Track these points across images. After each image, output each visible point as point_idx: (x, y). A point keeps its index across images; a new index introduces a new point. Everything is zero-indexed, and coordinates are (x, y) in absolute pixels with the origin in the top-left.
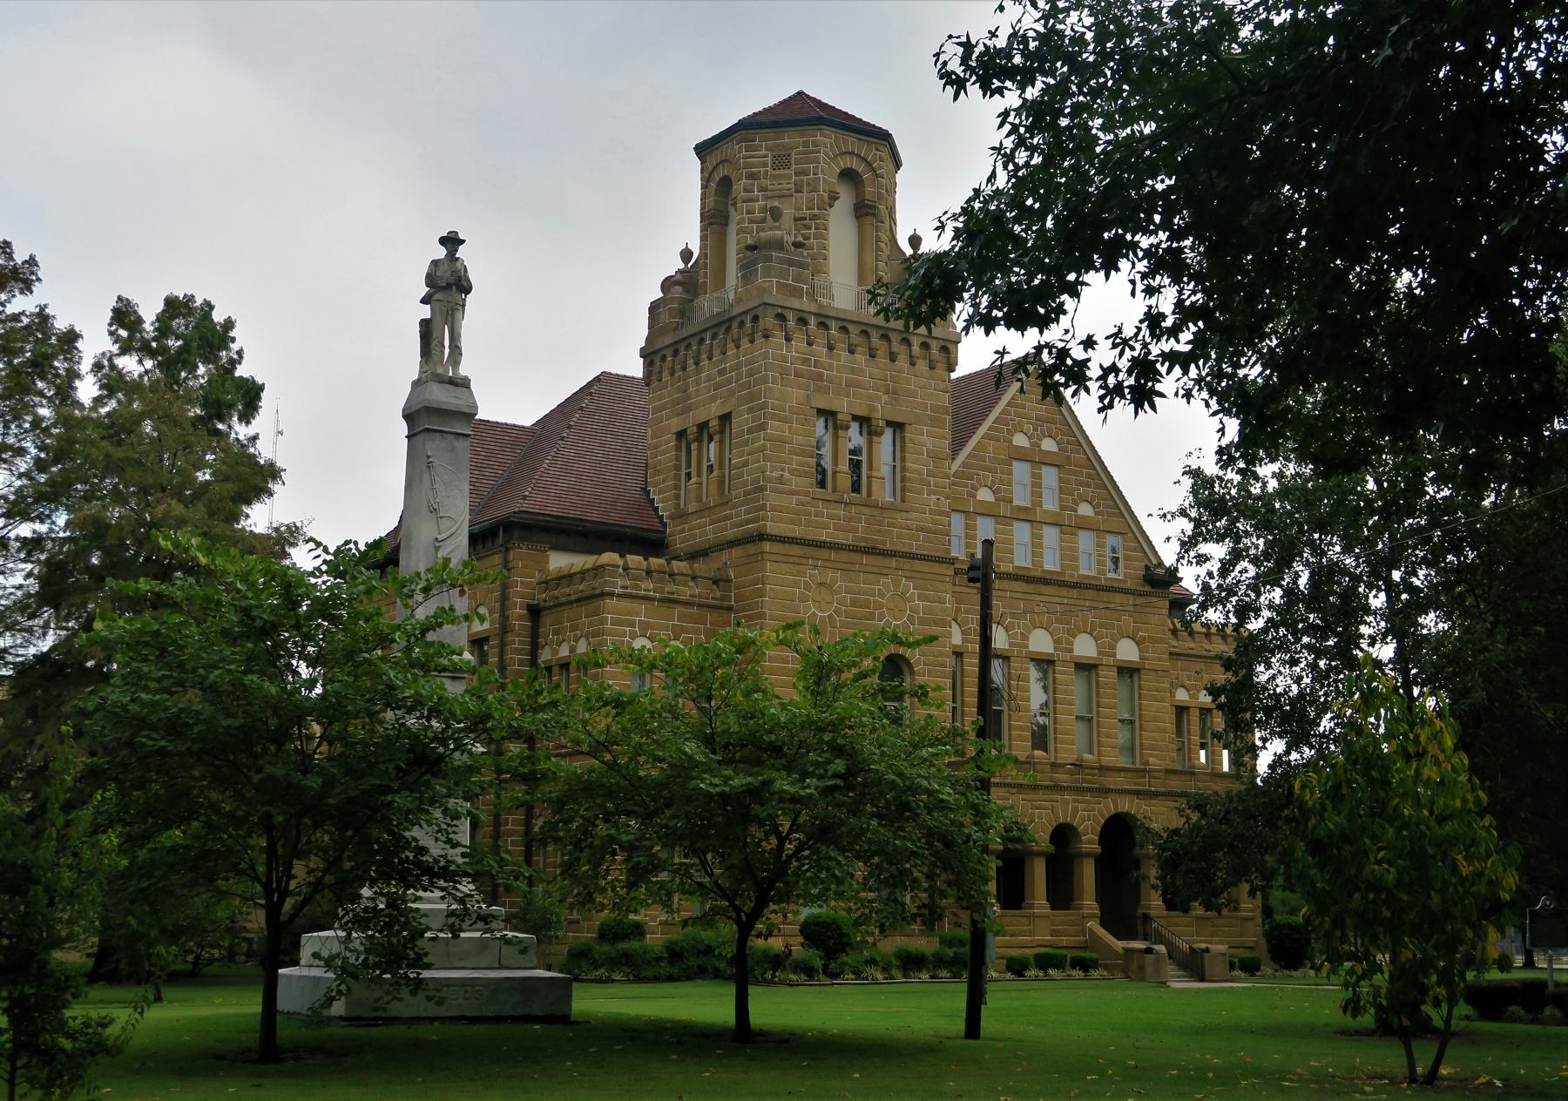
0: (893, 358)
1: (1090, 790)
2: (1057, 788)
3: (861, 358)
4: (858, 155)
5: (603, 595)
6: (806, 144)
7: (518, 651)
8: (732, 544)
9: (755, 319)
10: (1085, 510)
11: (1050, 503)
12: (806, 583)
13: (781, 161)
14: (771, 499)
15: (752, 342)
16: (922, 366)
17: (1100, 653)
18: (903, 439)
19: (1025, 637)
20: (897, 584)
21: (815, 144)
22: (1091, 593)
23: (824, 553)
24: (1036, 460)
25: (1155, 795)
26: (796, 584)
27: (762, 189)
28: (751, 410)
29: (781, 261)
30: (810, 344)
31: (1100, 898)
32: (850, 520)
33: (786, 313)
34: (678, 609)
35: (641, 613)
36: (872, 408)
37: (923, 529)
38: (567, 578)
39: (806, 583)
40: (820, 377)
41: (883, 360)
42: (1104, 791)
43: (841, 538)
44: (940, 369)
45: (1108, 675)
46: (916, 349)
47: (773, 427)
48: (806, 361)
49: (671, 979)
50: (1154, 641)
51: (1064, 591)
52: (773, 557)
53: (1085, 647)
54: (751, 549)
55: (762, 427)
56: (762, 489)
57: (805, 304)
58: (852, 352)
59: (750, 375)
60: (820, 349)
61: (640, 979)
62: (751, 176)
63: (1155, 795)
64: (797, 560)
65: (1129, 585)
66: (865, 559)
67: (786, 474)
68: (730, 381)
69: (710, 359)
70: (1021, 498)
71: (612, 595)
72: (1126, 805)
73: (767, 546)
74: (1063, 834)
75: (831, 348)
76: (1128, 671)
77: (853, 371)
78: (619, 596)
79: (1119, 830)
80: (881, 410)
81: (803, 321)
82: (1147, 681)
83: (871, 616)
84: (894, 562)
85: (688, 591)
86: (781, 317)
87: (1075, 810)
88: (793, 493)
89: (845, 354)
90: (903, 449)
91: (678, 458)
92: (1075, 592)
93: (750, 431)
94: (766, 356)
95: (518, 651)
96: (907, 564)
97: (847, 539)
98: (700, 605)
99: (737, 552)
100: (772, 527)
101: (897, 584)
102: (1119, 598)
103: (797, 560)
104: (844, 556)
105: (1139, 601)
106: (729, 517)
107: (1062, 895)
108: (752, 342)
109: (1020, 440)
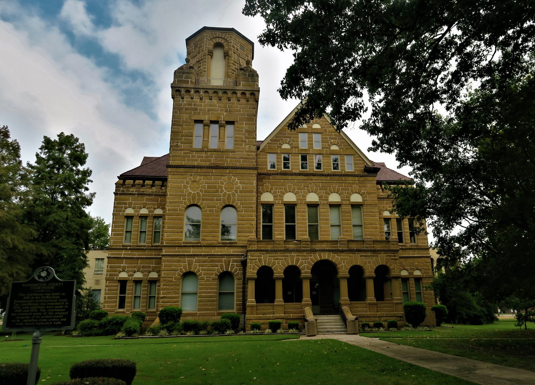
3: (215, 101)
4: (221, 38)
10: (334, 148)
12: (187, 182)
17: (342, 200)
20: (229, 179)
23: (196, 170)
25: (343, 251)
26: (182, 182)
30: (192, 98)
31: (312, 297)
32: (207, 157)
33: (180, 89)
34: (146, 197)
36: (219, 117)
37: (242, 158)
39: (187, 182)
41: (224, 101)
43: (203, 164)
51: (323, 178)
52: (172, 173)
57: (189, 85)
58: (211, 99)
63: (343, 251)
64: (183, 173)
65: (357, 173)
67: (179, 144)
72: (325, 256)
75: (201, 99)
76: (356, 206)
77: (211, 106)
78: (120, 194)
81: (188, 91)
83: (217, 191)
84: (228, 171)
85: (150, 191)
87: (298, 260)
88: (181, 150)
89: (208, 101)
96: (234, 171)
98: (155, 195)
101: (229, 179)
103: (183, 173)
104: (204, 170)
105: (361, 179)
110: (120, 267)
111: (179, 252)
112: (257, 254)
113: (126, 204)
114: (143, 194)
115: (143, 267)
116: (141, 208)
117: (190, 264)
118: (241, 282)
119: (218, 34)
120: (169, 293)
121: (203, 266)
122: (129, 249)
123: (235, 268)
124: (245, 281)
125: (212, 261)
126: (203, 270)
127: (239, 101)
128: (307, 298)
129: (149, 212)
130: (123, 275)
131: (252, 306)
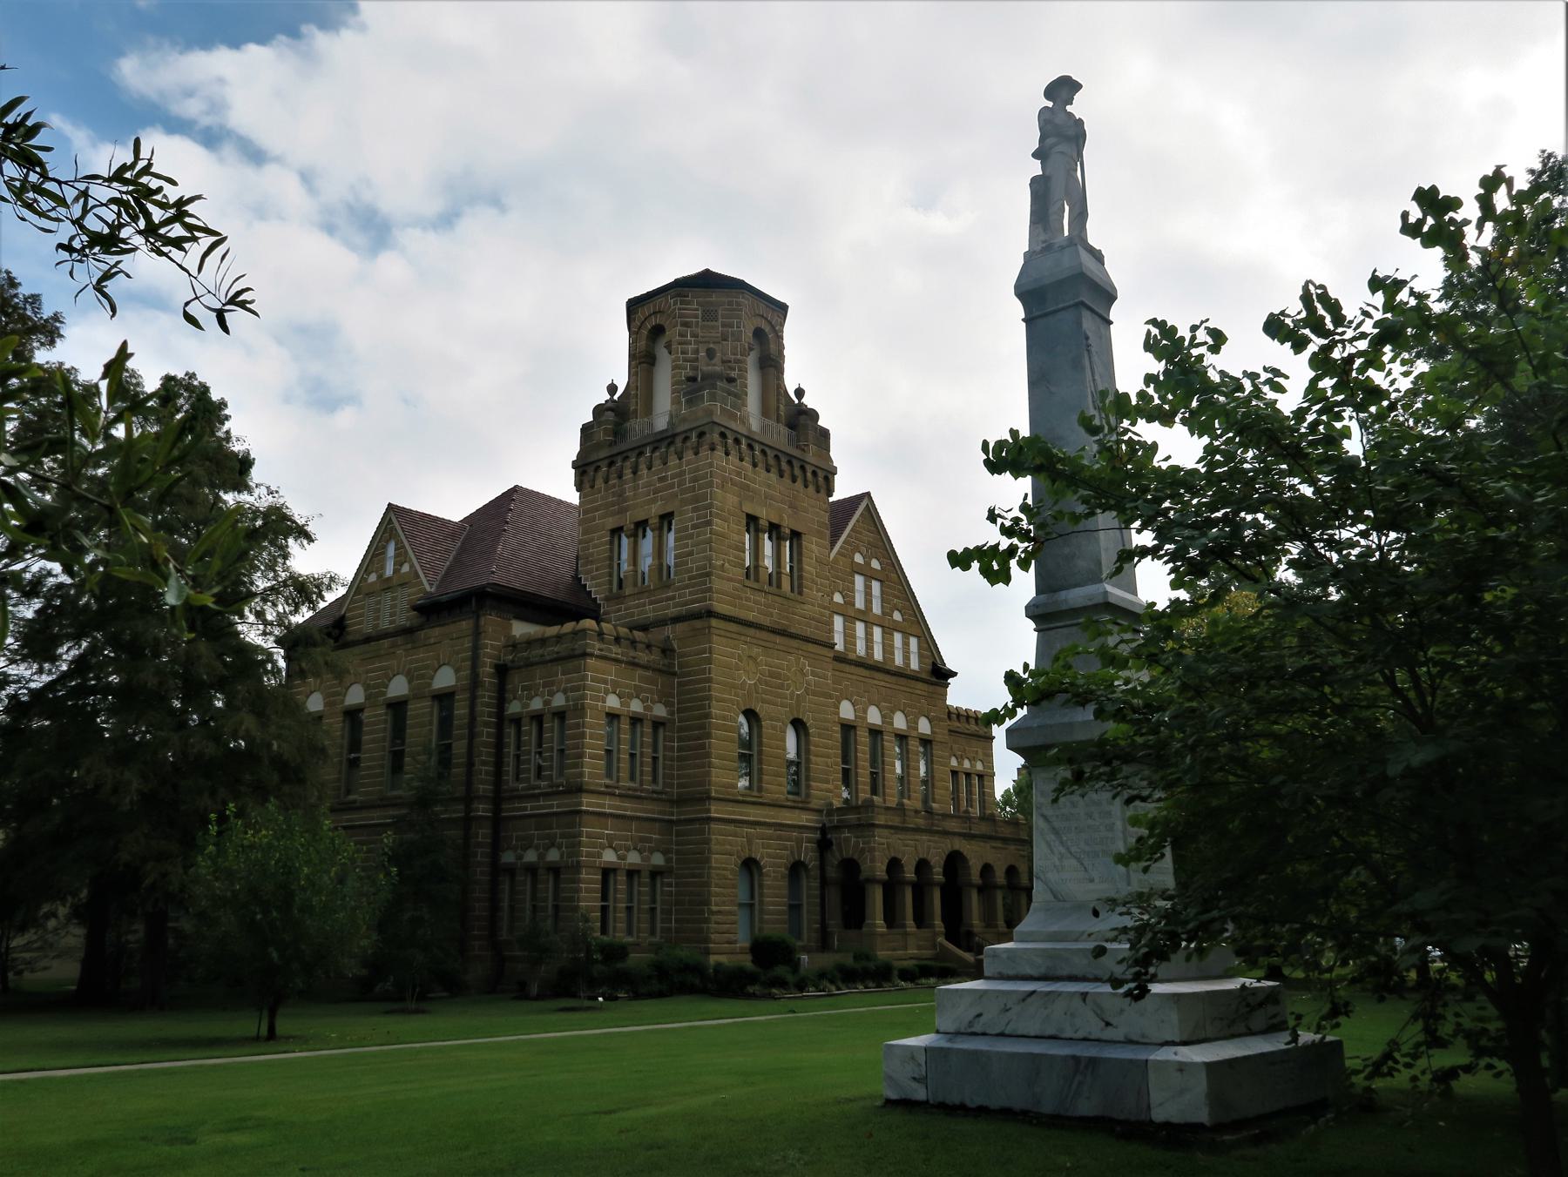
0: (794, 481)
1: (938, 832)
2: (917, 830)
3: (773, 476)
5: (585, 655)
6: (730, 303)
7: (487, 705)
8: (677, 619)
9: (701, 435)
11: (877, 609)
13: (709, 315)
14: (717, 584)
15: (696, 453)
16: (811, 489)
18: (800, 546)
19: (865, 712)
21: (738, 304)
22: (903, 681)
23: (752, 631)
24: (869, 576)
26: (732, 656)
27: (694, 335)
28: (695, 510)
29: (724, 390)
31: (943, 920)
32: (767, 606)
33: (728, 433)
34: (639, 672)
35: (612, 673)
36: (781, 518)
38: (530, 643)
40: (747, 488)
42: (946, 833)
44: (823, 494)
45: (914, 745)
46: (809, 475)
47: (718, 525)
48: (739, 474)
49: (660, 995)
50: (941, 720)
51: (888, 678)
53: (900, 722)
54: (698, 624)
55: (709, 523)
56: (708, 575)
58: (768, 471)
59: (694, 480)
60: (747, 465)
61: (637, 996)
62: (685, 324)
65: (924, 676)
66: (778, 639)
68: (672, 486)
69: (649, 468)
70: (860, 603)
71: (592, 655)
73: (714, 622)
74: (922, 866)
76: (926, 742)
77: (769, 486)
78: (598, 657)
79: (954, 861)
80: (788, 524)
82: (937, 751)
83: (781, 687)
84: (795, 643)
85: (643, 657)
86: (723, 435)
90: (800, 554)
91: (611, 550)
92: (894, 679)
93: (694, 527)
94: (711, 465)
95: (487, 705)
97: (767, 621)
98: (654, 670)
99: (680, 627)
100: (720, 607)
102: (920, 685)
105: (931, 688)
106: (673, 598)
107: (921, 920)
108: (696, 453)
109: (858, 559)
110: (600, 836)
111: (734, 813)
112: (886, 832)
113: (605, 682)
114: (634, 664)
115: (642, 840)
116: (630, 697)
117: (750, 842)
118: (816, 884)
119: (762, 308)
120: (724, 904)
121: (769, 847)
122: (620, 796)
123: (808, 855)
124: (824, 882)
125: (779, 838)
126: (769, 856)
127: (806, 486)
128: (938, 922)
129: (645, 708)
130: (609, 856)
131: (882, 935)
